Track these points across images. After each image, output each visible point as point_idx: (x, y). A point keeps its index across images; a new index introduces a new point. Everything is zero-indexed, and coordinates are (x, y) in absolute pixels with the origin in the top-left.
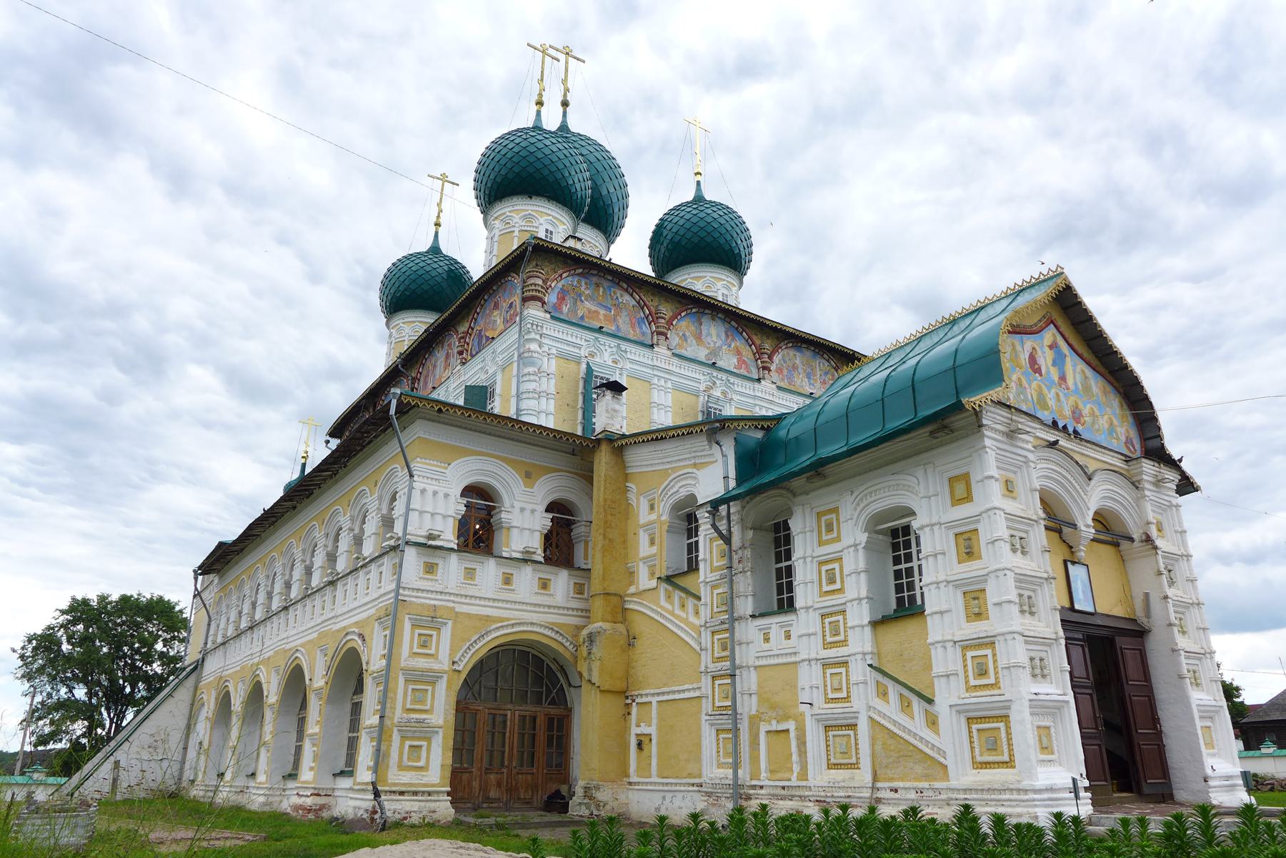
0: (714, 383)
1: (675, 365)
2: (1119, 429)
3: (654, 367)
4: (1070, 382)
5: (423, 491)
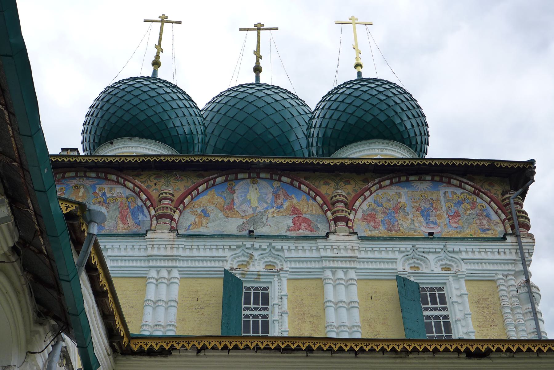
0: (251, 256)
1: (182, 248)
3: (148, 258)
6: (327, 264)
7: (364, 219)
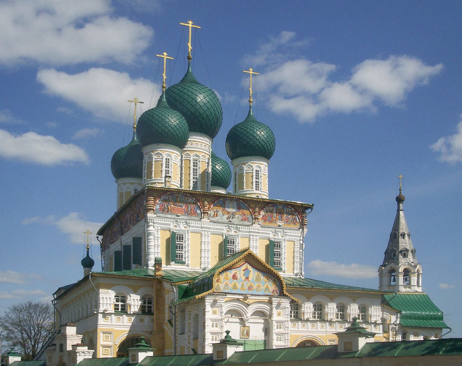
1: (212, 226)
2: (270, 289)
4: (250, 279)
5: (103, 298)
6: (251, 234)
7: (262, 218)
